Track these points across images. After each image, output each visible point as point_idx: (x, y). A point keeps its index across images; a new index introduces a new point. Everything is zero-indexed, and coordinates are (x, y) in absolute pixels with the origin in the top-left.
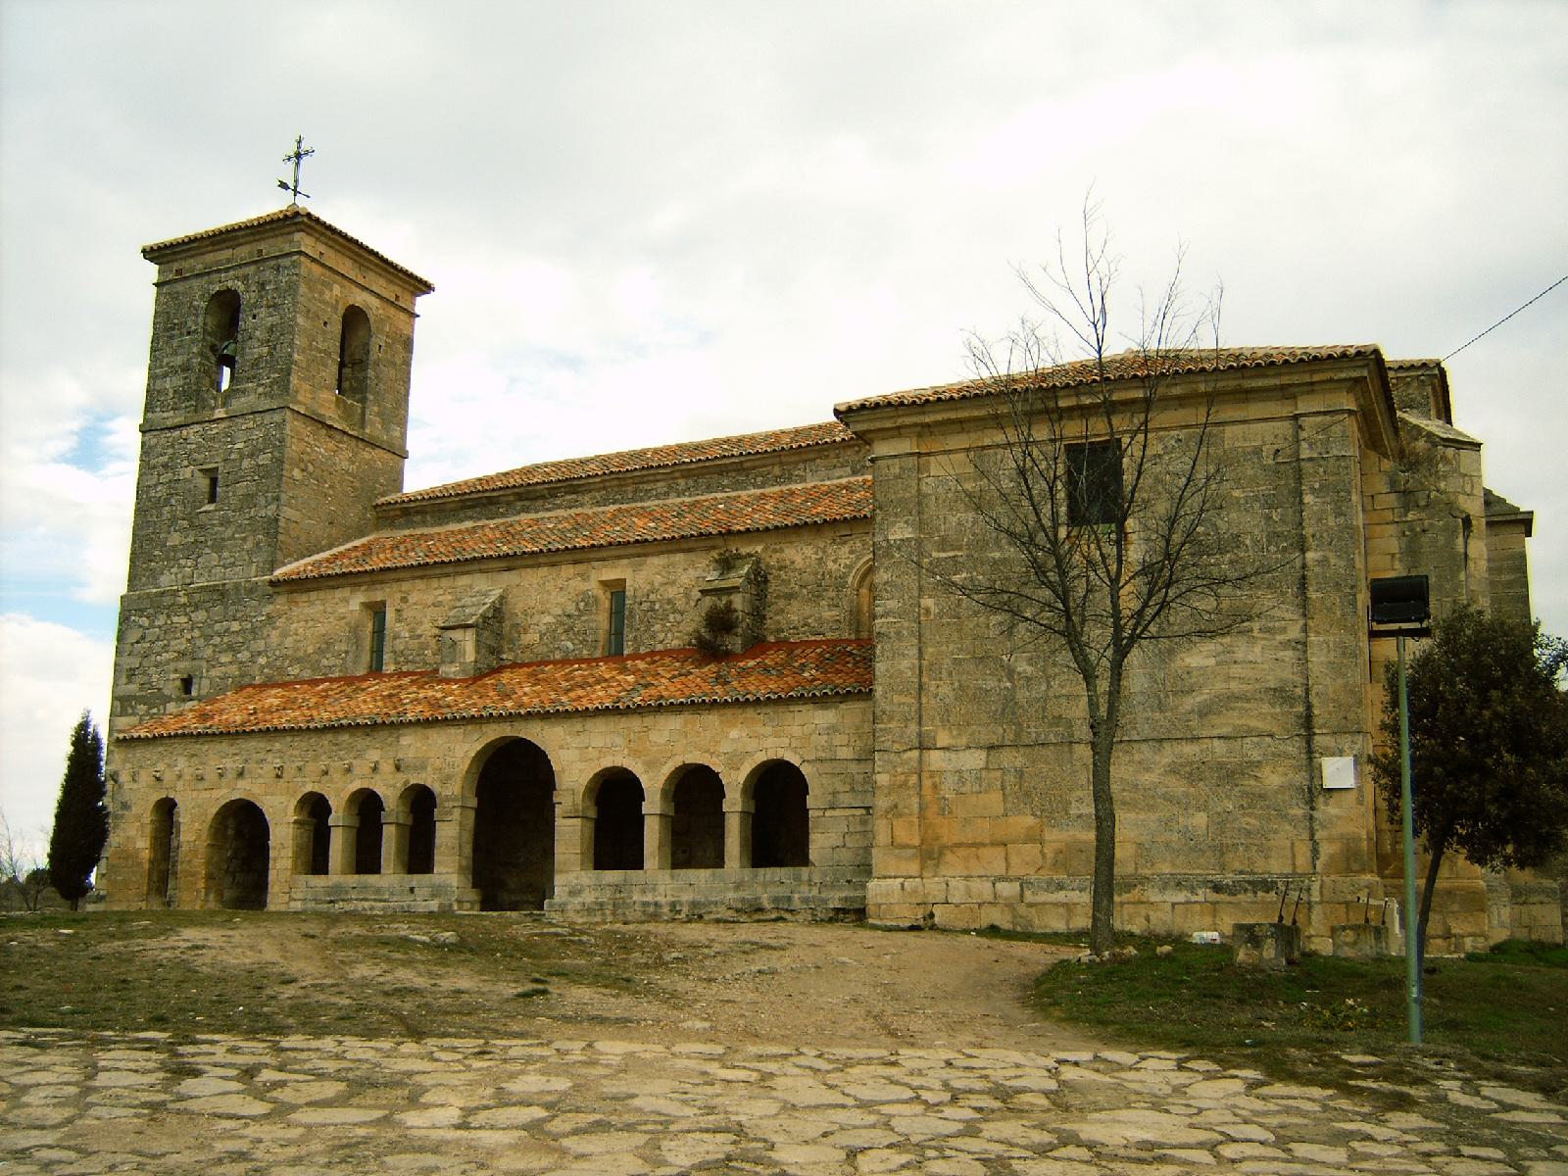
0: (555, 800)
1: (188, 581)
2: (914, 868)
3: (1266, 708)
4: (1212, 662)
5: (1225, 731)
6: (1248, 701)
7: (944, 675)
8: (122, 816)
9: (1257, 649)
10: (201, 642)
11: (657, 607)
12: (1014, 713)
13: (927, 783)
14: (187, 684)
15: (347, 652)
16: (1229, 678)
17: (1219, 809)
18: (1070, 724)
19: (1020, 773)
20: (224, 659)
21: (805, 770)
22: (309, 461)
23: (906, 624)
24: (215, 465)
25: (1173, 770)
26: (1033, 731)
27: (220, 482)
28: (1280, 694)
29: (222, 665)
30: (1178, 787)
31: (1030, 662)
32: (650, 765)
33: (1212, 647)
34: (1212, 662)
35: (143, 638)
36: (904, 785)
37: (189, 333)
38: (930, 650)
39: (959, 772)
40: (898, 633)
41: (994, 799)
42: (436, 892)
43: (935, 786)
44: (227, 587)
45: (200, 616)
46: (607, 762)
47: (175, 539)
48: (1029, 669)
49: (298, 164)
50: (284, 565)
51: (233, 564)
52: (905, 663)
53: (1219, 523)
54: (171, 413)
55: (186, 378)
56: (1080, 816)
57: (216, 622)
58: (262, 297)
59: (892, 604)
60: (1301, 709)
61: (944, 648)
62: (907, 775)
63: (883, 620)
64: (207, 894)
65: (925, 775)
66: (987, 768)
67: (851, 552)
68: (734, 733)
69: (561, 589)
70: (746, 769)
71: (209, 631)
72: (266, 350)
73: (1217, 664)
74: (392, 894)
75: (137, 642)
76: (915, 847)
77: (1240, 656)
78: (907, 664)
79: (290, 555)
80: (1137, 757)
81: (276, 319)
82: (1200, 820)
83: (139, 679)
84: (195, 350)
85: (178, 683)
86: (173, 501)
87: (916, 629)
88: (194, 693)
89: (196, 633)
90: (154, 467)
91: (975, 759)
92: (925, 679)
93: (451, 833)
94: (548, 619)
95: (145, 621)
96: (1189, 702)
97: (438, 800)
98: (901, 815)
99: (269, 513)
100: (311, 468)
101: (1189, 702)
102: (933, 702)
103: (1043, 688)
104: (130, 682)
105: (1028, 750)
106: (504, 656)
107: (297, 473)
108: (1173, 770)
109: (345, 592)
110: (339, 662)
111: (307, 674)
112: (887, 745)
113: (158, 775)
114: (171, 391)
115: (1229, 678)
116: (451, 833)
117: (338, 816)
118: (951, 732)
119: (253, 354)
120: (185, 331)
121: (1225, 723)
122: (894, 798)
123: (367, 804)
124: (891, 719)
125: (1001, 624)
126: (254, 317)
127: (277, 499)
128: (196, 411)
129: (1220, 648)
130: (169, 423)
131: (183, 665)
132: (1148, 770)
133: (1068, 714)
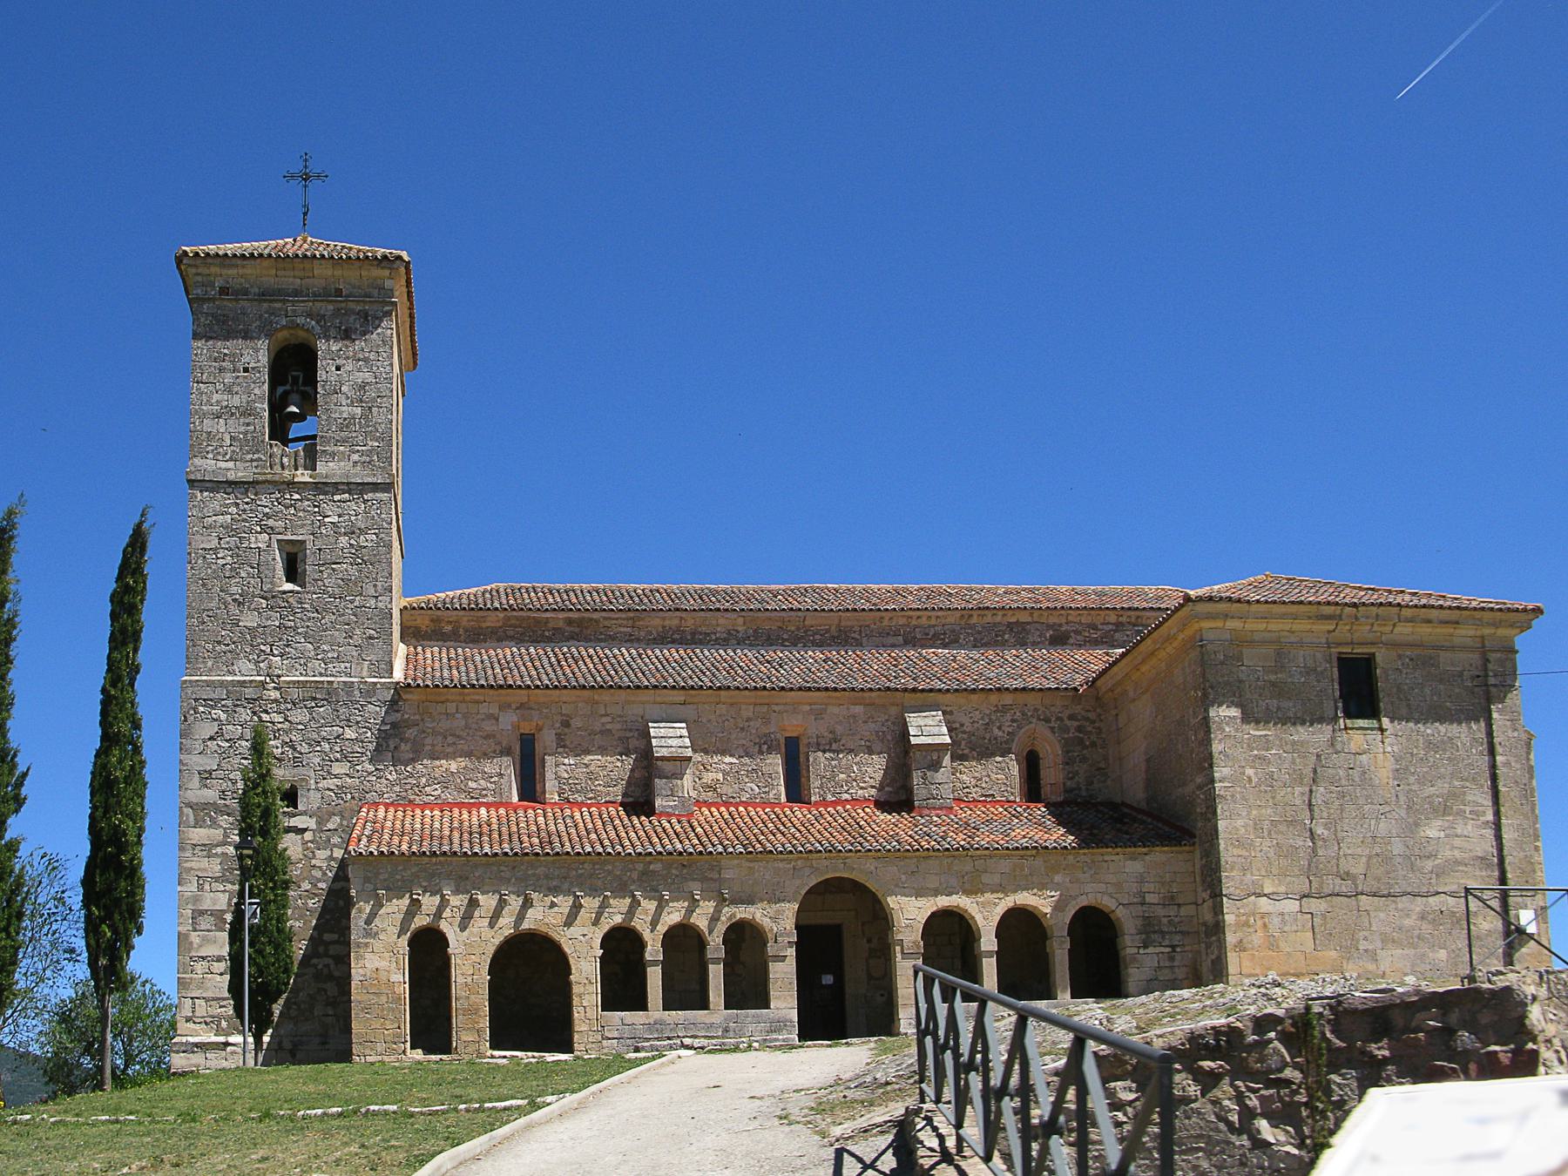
8: (366, 945)
9: (1470, 827)
10: (305, 748)
12: (1317, 868)
16: (1453, 848)
17: (1453, 947)
18: (1354, 878)
19: (1324, 916)
20: (337, 769)
26: (1332, 884)
29: (336, 776)
30: (1426, 928)
31: (1326, 826)
33: (1440, 823)
34: (1442, 834)
37: (246, 370)
39: (1282, 914)
40: (1233, 796)
43: (1265, 925)
44: (335, 685)
45: (299, 715)
47: (250, 620)
48: (1326, 832)
52: (1240, 823)
54: (231, 465)
55: (248, 424)
56: (1366, 951)
59: (1226, 771)
61: (1264, 811)
63: (1221, 784)
67: (1013, 721)
69: (742, 729)
71: (315, 736)
72: (359, 411)
73: (1447, 836)
75: (211, 738)
77: (1459, 831)
80: (1400, 906)
88: (300, 807)
91: (1292, 906)
96: (1429, 865)
115: (1453, 848)
118: (1273, 880)
123: (683, 941)
124: (1232, 869)
129: (1447, 825)
130: (231, 476)
133: (1353, 871)
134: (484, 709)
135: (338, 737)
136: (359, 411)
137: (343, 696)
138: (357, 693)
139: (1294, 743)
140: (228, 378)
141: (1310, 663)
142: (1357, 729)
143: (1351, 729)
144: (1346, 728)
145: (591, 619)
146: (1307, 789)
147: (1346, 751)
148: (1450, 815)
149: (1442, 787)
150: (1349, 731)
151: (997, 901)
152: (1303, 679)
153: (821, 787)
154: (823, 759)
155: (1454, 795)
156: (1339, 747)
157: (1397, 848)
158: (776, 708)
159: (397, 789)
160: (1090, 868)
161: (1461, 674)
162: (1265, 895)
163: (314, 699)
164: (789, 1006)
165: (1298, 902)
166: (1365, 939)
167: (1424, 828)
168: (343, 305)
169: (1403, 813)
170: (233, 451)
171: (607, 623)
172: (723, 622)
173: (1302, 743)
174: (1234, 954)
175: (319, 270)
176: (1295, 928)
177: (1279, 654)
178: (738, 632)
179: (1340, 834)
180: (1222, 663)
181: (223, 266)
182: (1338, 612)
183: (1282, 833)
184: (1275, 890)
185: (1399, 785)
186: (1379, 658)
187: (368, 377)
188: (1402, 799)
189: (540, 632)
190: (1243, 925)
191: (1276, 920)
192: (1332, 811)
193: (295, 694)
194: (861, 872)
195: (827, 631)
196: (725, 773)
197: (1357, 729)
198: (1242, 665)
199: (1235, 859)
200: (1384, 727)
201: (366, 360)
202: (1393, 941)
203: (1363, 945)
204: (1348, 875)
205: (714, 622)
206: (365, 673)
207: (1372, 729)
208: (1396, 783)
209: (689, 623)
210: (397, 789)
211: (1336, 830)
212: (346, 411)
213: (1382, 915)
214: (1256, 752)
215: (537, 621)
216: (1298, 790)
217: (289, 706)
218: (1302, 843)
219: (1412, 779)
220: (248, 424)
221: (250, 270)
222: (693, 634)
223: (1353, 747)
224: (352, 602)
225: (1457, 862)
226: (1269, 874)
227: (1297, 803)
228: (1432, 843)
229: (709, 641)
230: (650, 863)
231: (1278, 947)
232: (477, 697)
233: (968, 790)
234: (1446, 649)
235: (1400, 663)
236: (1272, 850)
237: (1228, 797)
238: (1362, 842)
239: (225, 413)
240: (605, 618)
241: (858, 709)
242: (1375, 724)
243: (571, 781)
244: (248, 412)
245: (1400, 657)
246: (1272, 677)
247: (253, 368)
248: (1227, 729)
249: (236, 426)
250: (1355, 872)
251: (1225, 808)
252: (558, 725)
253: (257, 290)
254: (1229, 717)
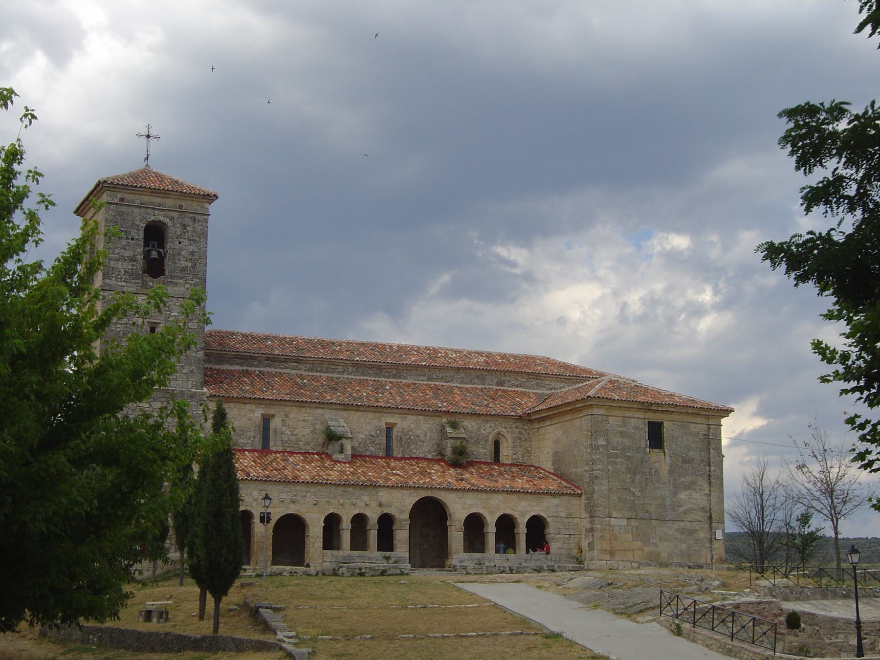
0: (448, 524)
3: (700, 513)
5: (690, 519)
6: (695, 510)
9: (698, 495)
16: (691, 503)
21: (548, 519)
24: (159, 321)
28: (703, 509)
37: (132, 239)
41: (629, 537)
44: (175, 392)
46: (473, 510)
54: (124, 284)
55: (133, 265)
60: (708, 515)
62: (606, 526)
68: (523, 504)
72: (189, 264)
77: (694, 497)
84: (138, 250)
93: (402, 536)
96: (681, 509)
98: (603, 540)
99: (199, 356)
101: (681, 509)
105: (639, 521)
109: (253, 407)
115: (691, 503)
116: (402, 536)
119: (181, 264)
121: (690, 517)
132: (671, 530)
136: (189, 264)
138: (186, 396)
140: (124, 242)
170: (126, 278)
187: (196, 249)
201: (194, 240)
206: (190, 387)
212: (184, 264)
213: (661, 529)
220: (133, 265)
225: (692, 509)
239: (122, 259)
244: (133, 259)
247: (136, 239)
249: (128, 266)
253: (139, 201)
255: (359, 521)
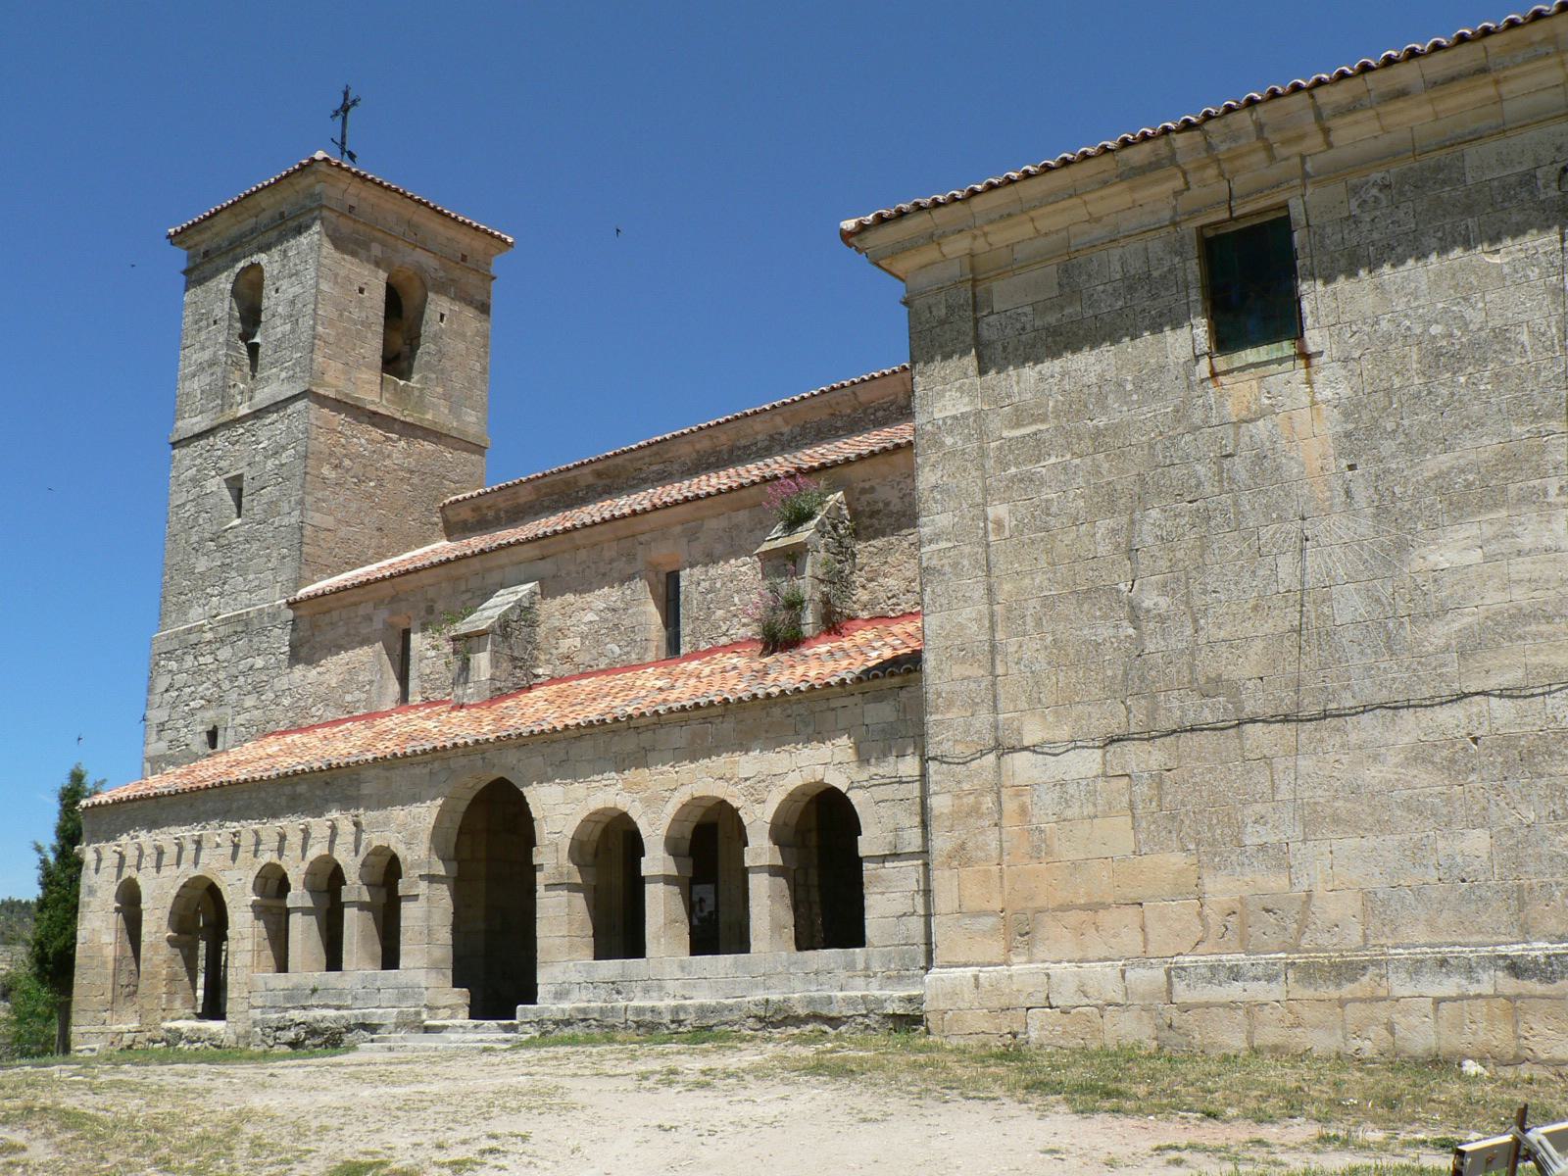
0: (536, 861)
1: (214, 612)
2: (995, 948)
4: (1476, 556)
5: (1510, 678)
6: (1549, 619)
7: (1030, 622)
10: (226, 685)
11: (718, 585)
12: (1142, 679)
13: (1010, 806)
14: (212, 737)
15: (371, 682)
16: (1508, 584)
17: (1511, 821)
18: (1234, 690)
19: (1158, 781)
20: (249, 702)
22: (345, 456)
23: (967, 549)
25: (1419, 756)
26: (1177, 708)
27: (244, 493)
29: (247, 710)
30: (1426, 782)
31: (1164, 589)
32: (648, 803)
33: (1474, 530)
34: (1476, 556)
35: (171, 685)
36: (975, 811)
37: (215, 322)
38: (1007, 587)
39: (1062, 784)
40: (955, 565)
42: (404, 993)
43: (1023, 811)
44: (251, 615)
45: (225, 653)
47: (201, 565)
48: (1164, 603)
49: (344, 119)
50: (314, 582)
51: (259, 587)
52: (969, 612)
53: (1469, 314)
54: (199, 418)
55: (212, 374)
56: (1263, 847)
57: (242, 659)
58: (284, 266)
59: (944, 520)
61: (1027, 581)
63: (934, 547)
64: (170, 1001)
65: (1005, 794)
66: (1105, 775)
69: (604, 575)
70: (775, 799)
72: (288, 327)
74: (355, 998)
75: (167, 691)
76: (994, 913)
77: (1527, 541)
78: (969, 616)
79: (322, 571)
80: (1354, 738)
81: (297, 289)
82: (1477, 841)
83: (168, 735)
85: (204, 737)
86: (201, 521)
87: (982, 558)
89: (222, 675)
90: (183, 483)
91: (1088, 762)
92: (999, 636)
94: (591, 617)
95: (173, 665)
96: (1440, 633)
97: (403, 868)
98: (967, 862)
99: (293, 520)
100: (347, 463)
102: (1014, 669)
103: (1189, 631)
104: (159, 739)
106: (540, 671)
107: (326, 470)
108: (1419, 756)
110: (363, 696)
111: (330, 716)
112: (946, 746)
113: (119, 849)
114: (199, 392)
115: (1508, 584)
117: (354, 889)
118: (1044, 717)
120: (211, 321)
122: (959, 834)
124: (950, 705)
125: (1114, 532)
126: (277, 291)
127: (301, 502)
128: (222, 411)
129: (1489, 531)
130: (197, 430)
131: (210, 715)
132: (1375, 758)
133: (1232, 673)
134: (362, 611)
135: (251, 669)
137: (256, 625)
139: (1098, 433)
140: (203, 336)
141: (1136, 266)
142: (1241, 369)
143: (1226, 373)
144: (1214, 375)
145: (617, 466)
146: (1125, 519)
147: (1214, 422)
148: (1496, 506)
149: (1484, 447)
150: (1222, 379)
151: (667, 794)
152: (1120, 303)
153: (693, 632)
154: (696, 595)
155: (1511, 461)
156: (1197, 417)
157: (1349, 606)
158: (642, 538)
159: (290, 714)
160: (807, 725)
161: (1528, 180)
162: (1026, 749)
163: (236, 632)
164: (418, 965)
165: (1100, 752)
166: (1260, 820)
167: (1423, 551)
168: (283, 227)
169: (1365, 526)
171: (638, 465)
172: (759, 426)
173: (1115, 429)
174: (947, 873)
175: (264, 200)
176: (1089, 810)
177: (1066, 270)
178: (782, 434)
179: (1198, 602)
180: (942, 322)
181: (200, 232)
182: (1164, 151)
183: (1067, 619)
184: (1048, 736)
185: (1352, 467)
186: (1296, 211)
188: (1362, 495)
189: (574, 494)
190: (968, 815)
191: (1049, 798)
192: (1180, 554)
193: (222, 631)
194: (505, 767)
195: (892, 403)
196: (583, 637)
197: (1241, 369)
198: (992, 313)
199: (957, 687)
200: (1312, 348)
202: (1336, 820)
203: (1251, 839)
204: (1214, 686)
205: (749, 431)
207: (1280, 361)
208: (1344, 463)
209: (723, 439)
210: (290, 714)
211: (1189, 594)
214: (1013, 470)
215: (567, 483)
216: (1104, 525)
217: (218, 645)
218: (1111, 632)
219: (1388, 447)
221: (220, 223)
222: (731, 451)
223: (1232, 410)
224: (273, 523)
225: (1521, 616)
226: (1034, 702)
227: (1102, 550)
228: (1447, 579)
229: (750, 455)
230: (297, 784)
231: (1049, 853)
232: (352, 600)
233: (894, 600)
234: (1477, 137)
235: (1354, 203)
236: (1042, 656)
237: (947, 569)
238: (1255, 608)
240: (631, 461)
241: (742, 516)
242: (1287, 348)
243: (432, 677)
245: (1354, 191)
246: (1052, 319)
248: (949, 441)
250: (1234, 676)
251: (938, 590)
252: (422, 613)
254: (954, 417)
255: (328, 880)
